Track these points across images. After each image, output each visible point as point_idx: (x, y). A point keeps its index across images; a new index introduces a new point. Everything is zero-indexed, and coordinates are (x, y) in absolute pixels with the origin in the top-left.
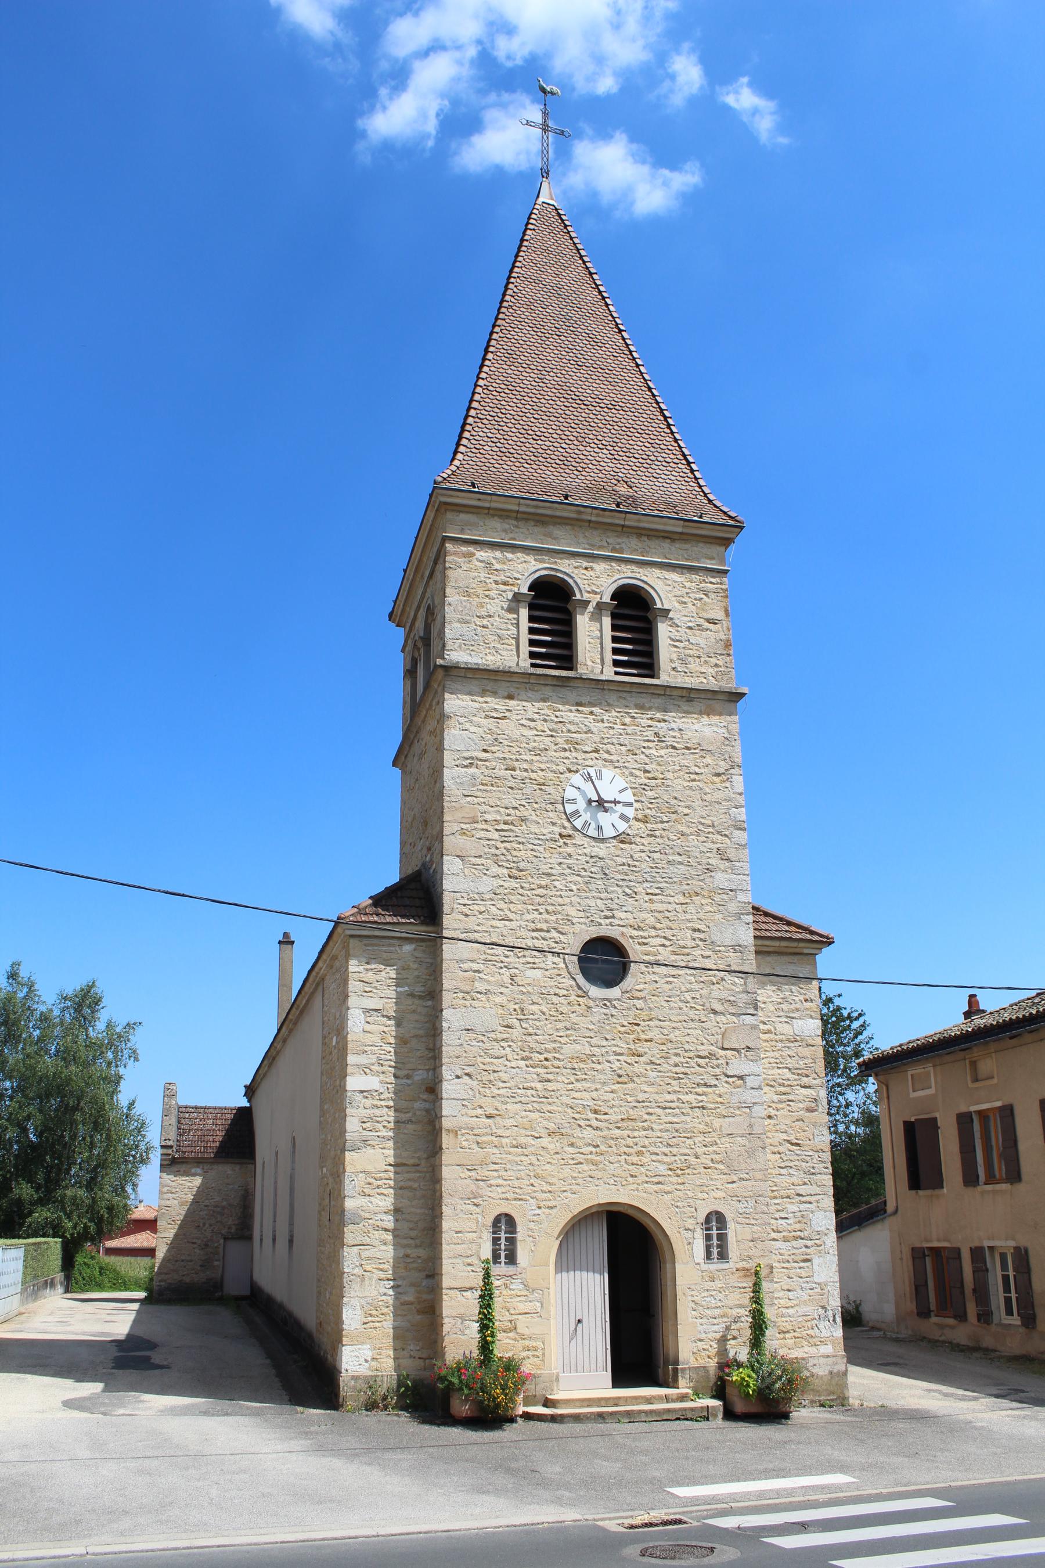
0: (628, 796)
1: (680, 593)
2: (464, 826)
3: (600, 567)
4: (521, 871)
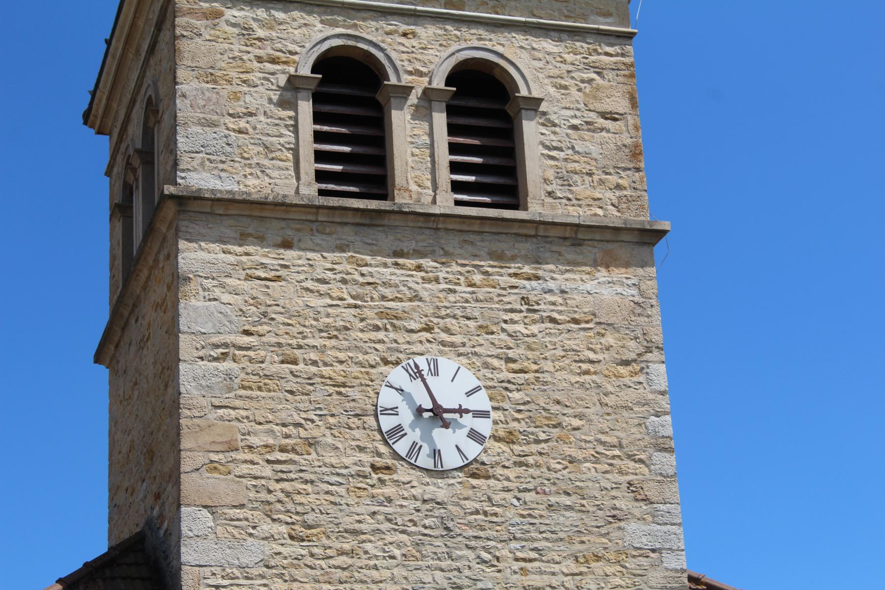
0: (481, 401)
1: (557, 72)
2: (214, 457)
3: (427, 32)
4: (310, 527)
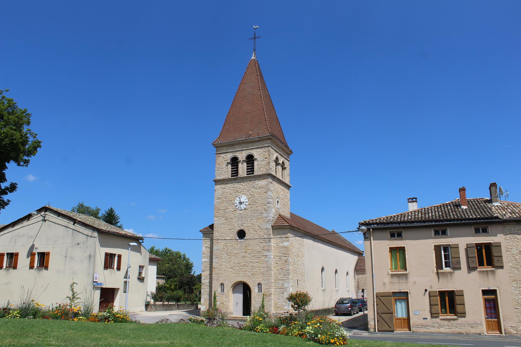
0: (247, 200)
3: (243, 152)
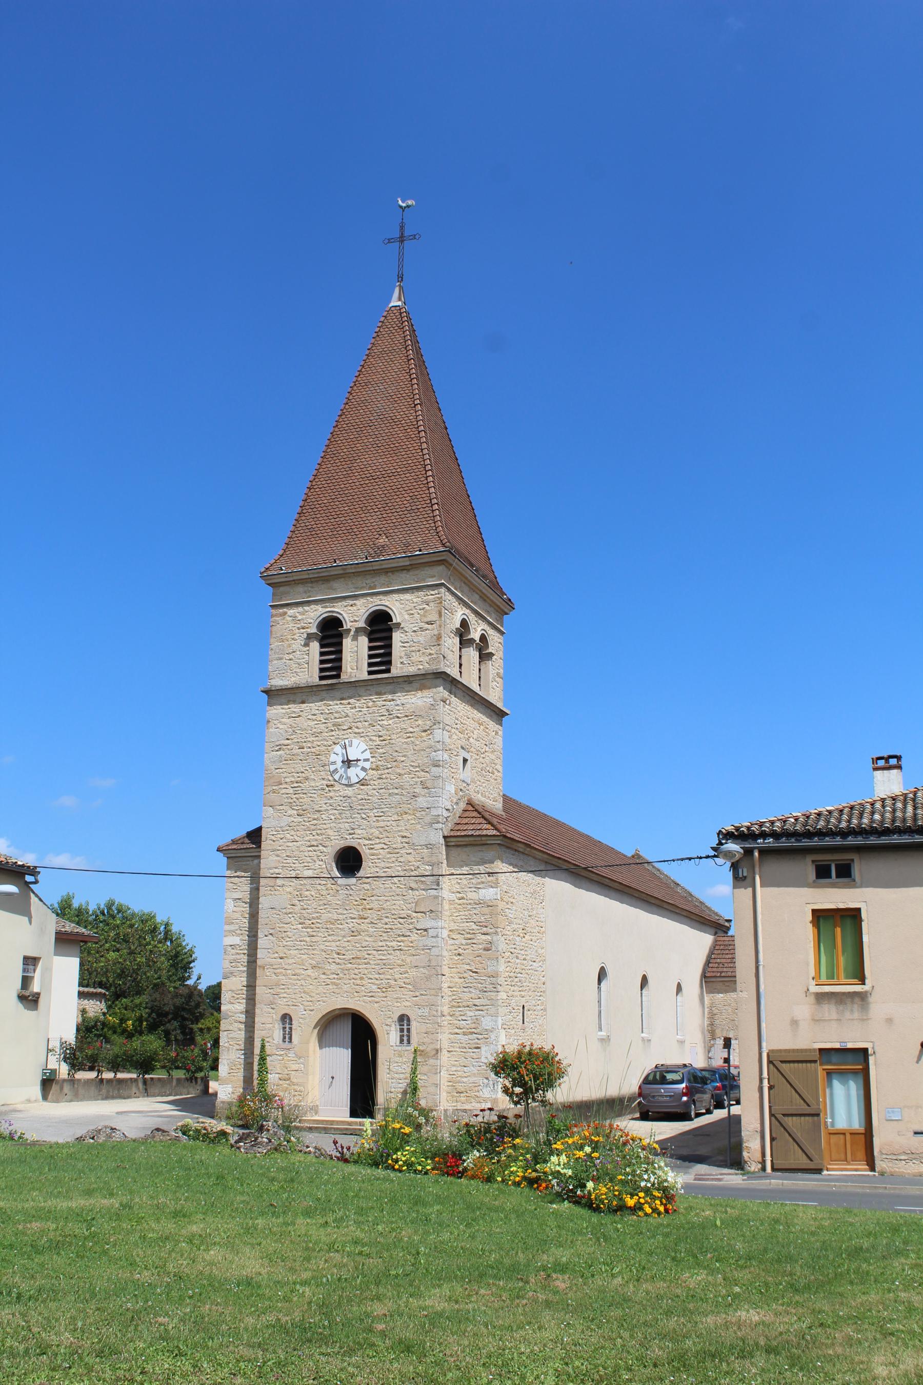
0: (367, 755)
3: (360, 602)
